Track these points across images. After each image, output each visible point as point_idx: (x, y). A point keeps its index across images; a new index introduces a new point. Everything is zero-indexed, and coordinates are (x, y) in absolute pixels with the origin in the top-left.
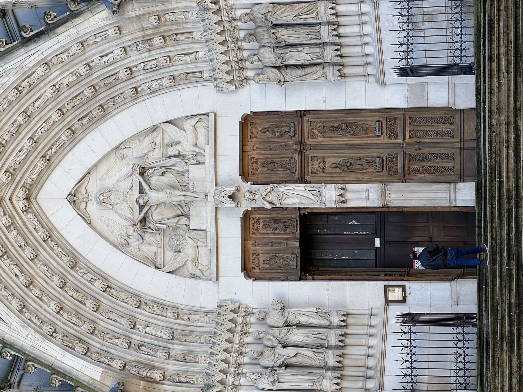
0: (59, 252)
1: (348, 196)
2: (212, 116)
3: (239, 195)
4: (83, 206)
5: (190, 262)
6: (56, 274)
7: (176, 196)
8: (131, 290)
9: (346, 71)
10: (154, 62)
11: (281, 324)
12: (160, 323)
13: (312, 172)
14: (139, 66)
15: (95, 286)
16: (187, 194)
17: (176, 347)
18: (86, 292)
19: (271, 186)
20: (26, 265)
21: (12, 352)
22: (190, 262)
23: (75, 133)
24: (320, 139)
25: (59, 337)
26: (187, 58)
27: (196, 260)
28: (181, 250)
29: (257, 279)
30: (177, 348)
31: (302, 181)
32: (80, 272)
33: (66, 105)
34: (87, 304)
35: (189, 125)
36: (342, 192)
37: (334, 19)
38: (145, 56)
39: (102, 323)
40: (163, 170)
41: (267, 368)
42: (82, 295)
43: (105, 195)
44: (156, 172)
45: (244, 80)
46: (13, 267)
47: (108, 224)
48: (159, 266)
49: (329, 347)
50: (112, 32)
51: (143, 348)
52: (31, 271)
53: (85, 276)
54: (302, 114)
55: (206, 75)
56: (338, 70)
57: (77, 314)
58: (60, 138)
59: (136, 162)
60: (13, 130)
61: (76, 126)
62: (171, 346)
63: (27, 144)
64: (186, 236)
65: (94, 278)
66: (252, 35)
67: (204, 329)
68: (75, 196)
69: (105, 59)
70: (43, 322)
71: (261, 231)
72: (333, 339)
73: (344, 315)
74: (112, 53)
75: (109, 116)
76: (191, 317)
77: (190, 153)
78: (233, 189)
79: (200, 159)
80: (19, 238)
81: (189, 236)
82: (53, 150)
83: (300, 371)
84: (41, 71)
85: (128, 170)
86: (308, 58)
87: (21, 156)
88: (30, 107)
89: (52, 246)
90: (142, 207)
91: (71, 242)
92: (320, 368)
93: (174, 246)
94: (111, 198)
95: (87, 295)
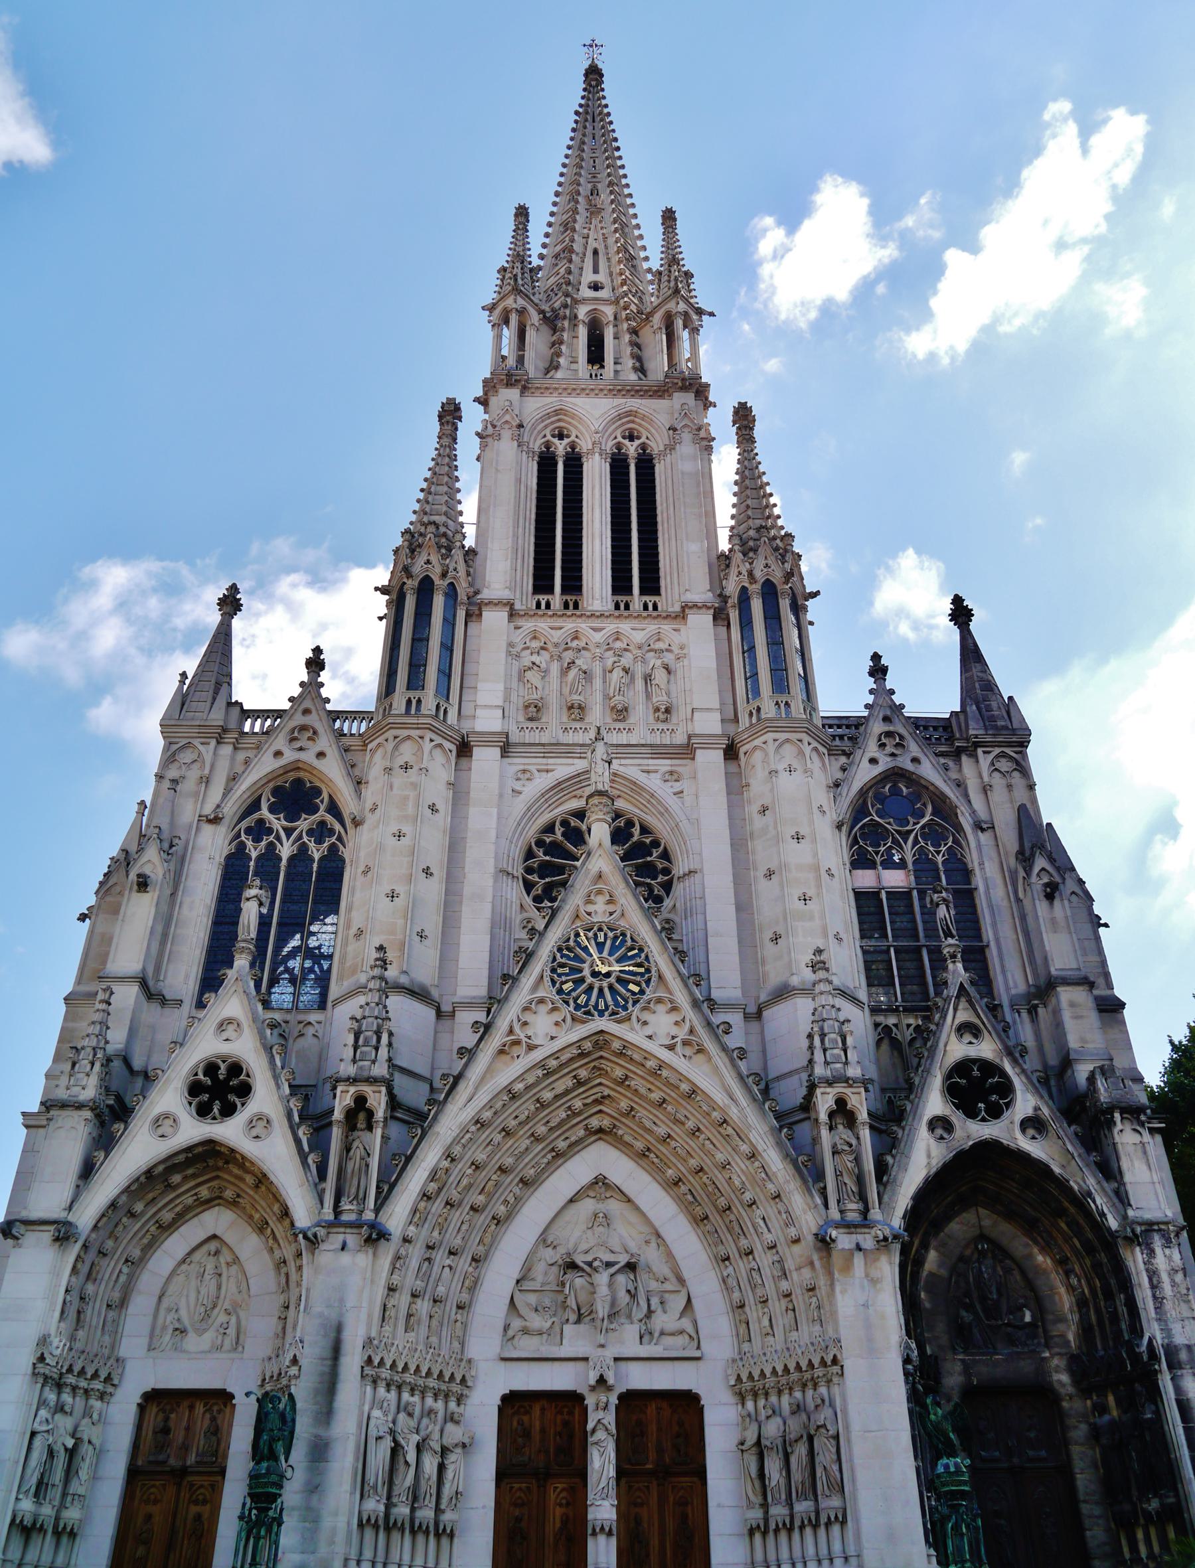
1: (602, 1538)
2: (697, 1354)
3: (603, 1389)
4: (592, 1194)
5: (524, 1323)
9: (758, 1537)
10: (760, 1282)
11: (445, 1444)
12: (454, 1284)
13: (630, 1487)
14: (753, 1263)
17: (426, 1303)
19: (614, 1431)
20: (527, 1127)
21: (432, 1113)
22: (524, 1323)
24: (671, 1499)
25: (446, 1164)
26: (766, 1322)
27: (525, 1331)
29: (500, 1410)
30: (423, 1307)
31: (620, 1473)
35: (686, 1324)
36: (607, 1529)
37: (823, 1520)
38: (766, 1272)
39: (458, 1213)
40: (633, 1291)
41: (394, 1422)
45: (742, 1398)
46: (526, 1113)
49: (413, 1510)
50: (792, 1232)
51: (426, 1263)
52: (521, 1133)
54: (701, 1473)
55: (746, 1347)
56: (758, 1526)
57: (470, 1185)
59: (642, 1259)
60: (679, 1116)
61: (683, 1187)
62: (427, 1298)
63: (661, 1131)
66: (797, 1409)
67: (443, 1341)
69: (762, 1223)
70: (464, 1146)
71: (559, 1417)
72: (426, 1514)
73: (452, 1530)
74: (769, 1231)
76: (459, 1324)
78: (611, 1381)
80: (558, 1120)
82: (656, 1160)
83: (387, 1468)
84: (745, 1148)
85: (633, 1246)
86: (773, 1483)
87: (648, 1124)
88: (703, 1136)
90: (590, 1264)
91: (550, 1179)
92: (389, 1497)
95: (490, 1196)
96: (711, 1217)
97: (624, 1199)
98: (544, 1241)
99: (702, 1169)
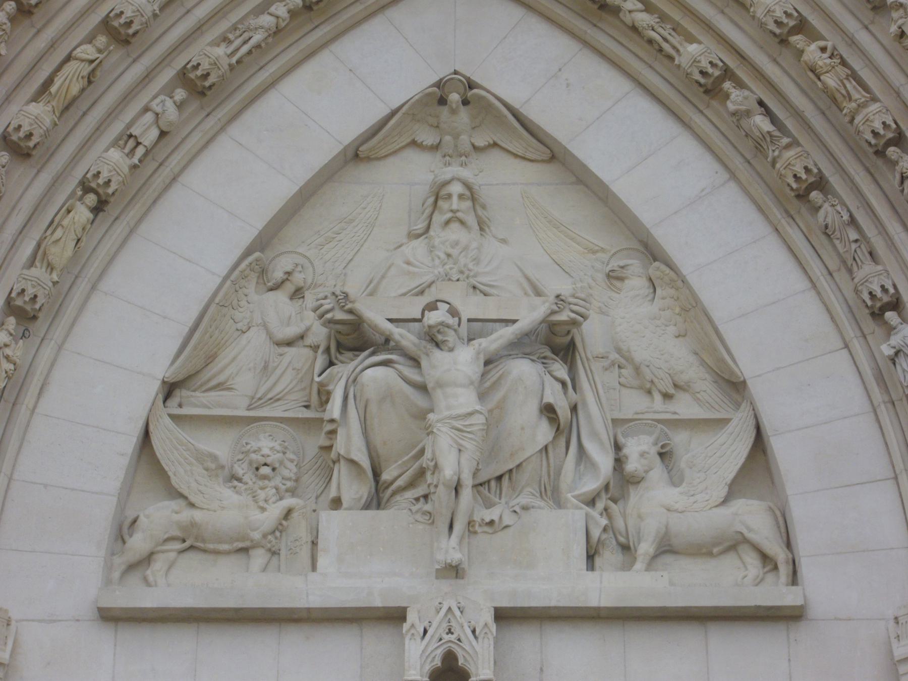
0: (246, 35)
2: (788, 597)
4: (428, 137)
5: (187, 515)
6: (162, 9)
7: (454, 453)
8: (83, 286)
15: (107, 150)
16: (467, 493)
18: (84, 114)
23: (706, 98)
28: (236, 483)
32: (163, 101)
33: (822, 43)
34: (35, 109)
40: (563, 412)
42: (75, 90)
43: (469, 203)
44: (558, 386)
47: (352, 221)
48: (173, 402)
53: (149, 117)
58: (691, 39)
61: (736, 95)
64: (289, 502)
65: (140, 151)
68: (465, 102)
75: (777, 213)
77: (631, 522)
79: (609, 556)
81: (295, 515)
89: (272, 9)
91: (289, 86)
93: (253, 456)
94: (455, 226)
96: (834, 180)
97: (535, 150)
98: (263, 272)
99: (802, 26)
